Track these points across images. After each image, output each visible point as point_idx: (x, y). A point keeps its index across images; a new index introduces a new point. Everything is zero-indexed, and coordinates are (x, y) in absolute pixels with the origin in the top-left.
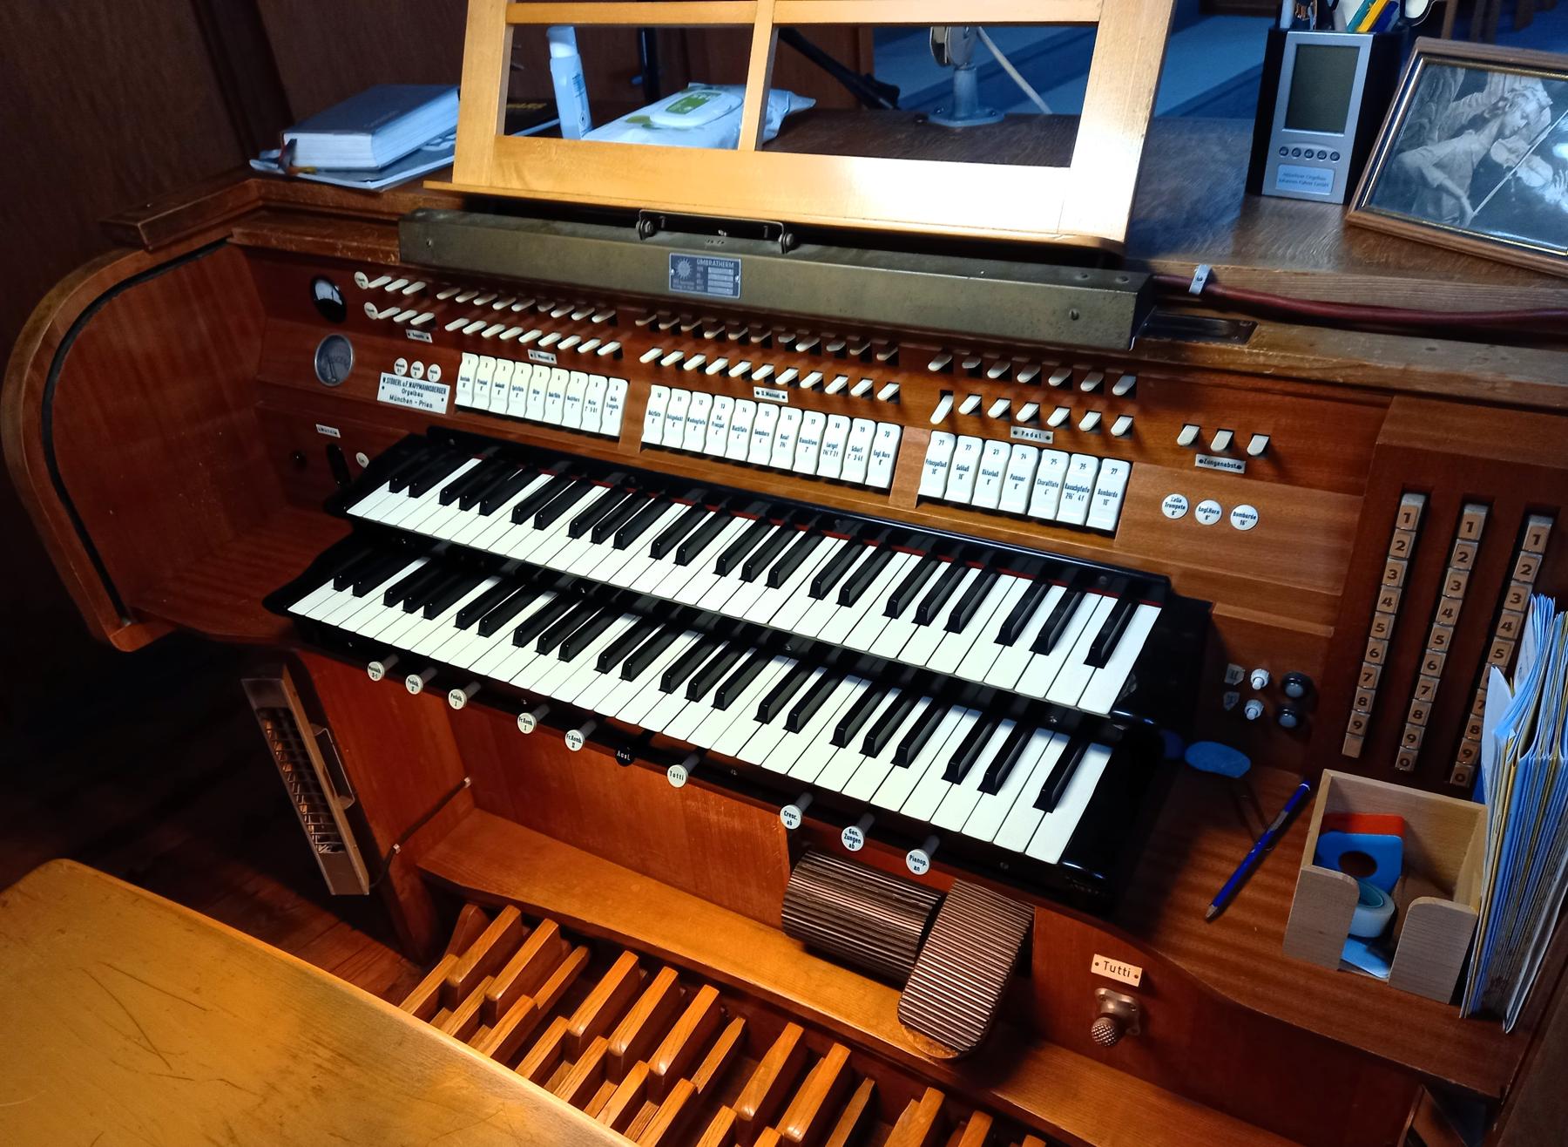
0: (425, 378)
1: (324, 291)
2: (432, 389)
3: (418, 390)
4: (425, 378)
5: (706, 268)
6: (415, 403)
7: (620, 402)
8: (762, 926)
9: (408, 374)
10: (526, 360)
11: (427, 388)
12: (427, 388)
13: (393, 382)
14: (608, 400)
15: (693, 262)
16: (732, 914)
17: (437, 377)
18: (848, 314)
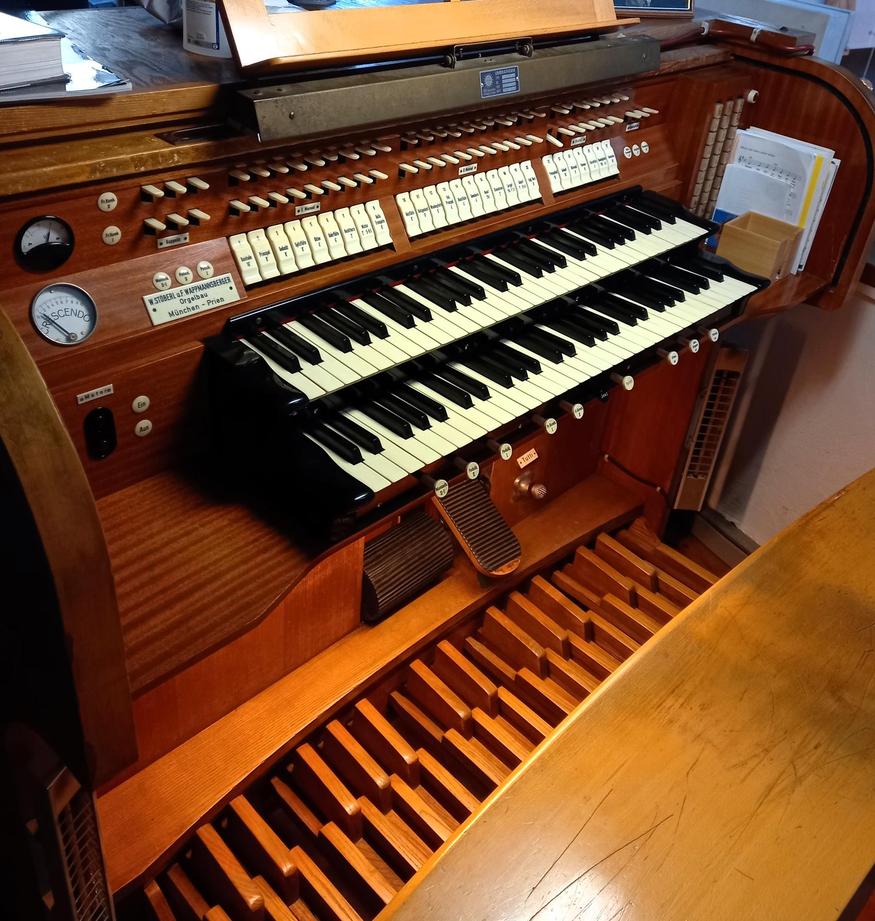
0: (197, 277)
1: (35, 237)
2: (215, 284)
3: (199, 293)
4: (197, 277)
5: (501, 76)
6: (203, 306)
7: (383, 217)
8: (337, 644)
9: (176, 283)
10: (294, 217)
11: (208, 286)
12: (208, 286)
13: (164, 298)
14: (374, 219)
15: (493, 74)
16: (315, 659)
17: (211, 271)
18: (570, 84)
